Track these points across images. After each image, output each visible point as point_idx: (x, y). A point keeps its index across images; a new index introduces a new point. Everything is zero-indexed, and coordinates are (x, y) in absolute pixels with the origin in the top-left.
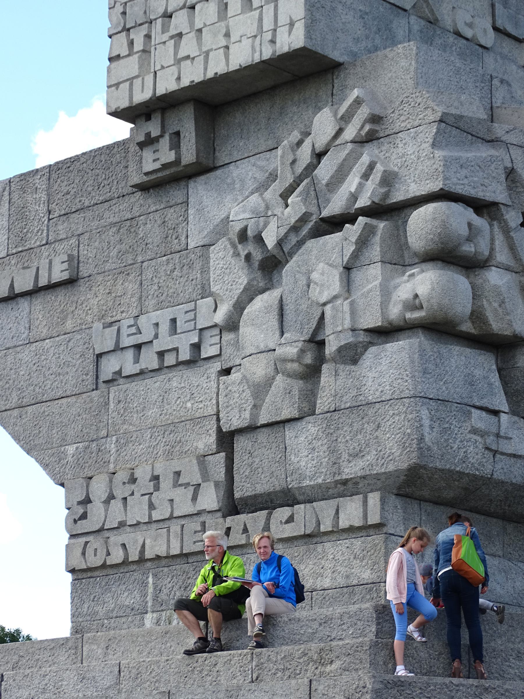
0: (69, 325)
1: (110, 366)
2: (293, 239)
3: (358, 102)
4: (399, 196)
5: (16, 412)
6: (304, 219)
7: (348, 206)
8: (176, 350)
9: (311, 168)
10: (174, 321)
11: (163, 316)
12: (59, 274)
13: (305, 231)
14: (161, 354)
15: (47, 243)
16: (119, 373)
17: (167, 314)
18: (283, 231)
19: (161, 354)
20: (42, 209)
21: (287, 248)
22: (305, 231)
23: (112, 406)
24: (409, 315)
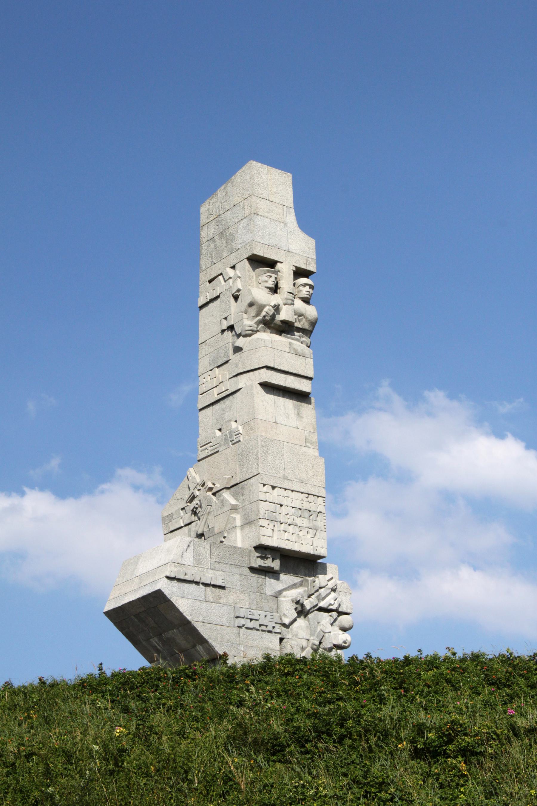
0: (221, 601)
1: (242, 622)
2: (313, 609)
3: (332, 578)
4: (340, 610)
5: (202, 623)
6: (317, 605)
7: (328, 606)
8: (266, 626)
9: (317, 591)
10: (265, 616)
11: (263, 614)
12: (220, 583)
13: (316, 608)
14: (260, 625)
15: (210, 569)
16: (244, 625)
17: (265, 613)
18: (312, 606)
19: (260, 625)
20: (208, 556)
21: (310, 611)
22: (316, 608)
23: (241, 635)
24: (343, 644)
